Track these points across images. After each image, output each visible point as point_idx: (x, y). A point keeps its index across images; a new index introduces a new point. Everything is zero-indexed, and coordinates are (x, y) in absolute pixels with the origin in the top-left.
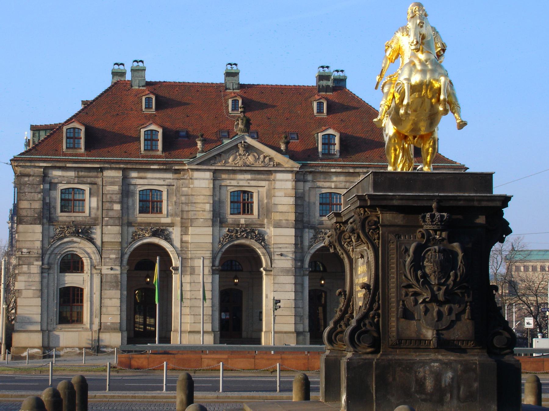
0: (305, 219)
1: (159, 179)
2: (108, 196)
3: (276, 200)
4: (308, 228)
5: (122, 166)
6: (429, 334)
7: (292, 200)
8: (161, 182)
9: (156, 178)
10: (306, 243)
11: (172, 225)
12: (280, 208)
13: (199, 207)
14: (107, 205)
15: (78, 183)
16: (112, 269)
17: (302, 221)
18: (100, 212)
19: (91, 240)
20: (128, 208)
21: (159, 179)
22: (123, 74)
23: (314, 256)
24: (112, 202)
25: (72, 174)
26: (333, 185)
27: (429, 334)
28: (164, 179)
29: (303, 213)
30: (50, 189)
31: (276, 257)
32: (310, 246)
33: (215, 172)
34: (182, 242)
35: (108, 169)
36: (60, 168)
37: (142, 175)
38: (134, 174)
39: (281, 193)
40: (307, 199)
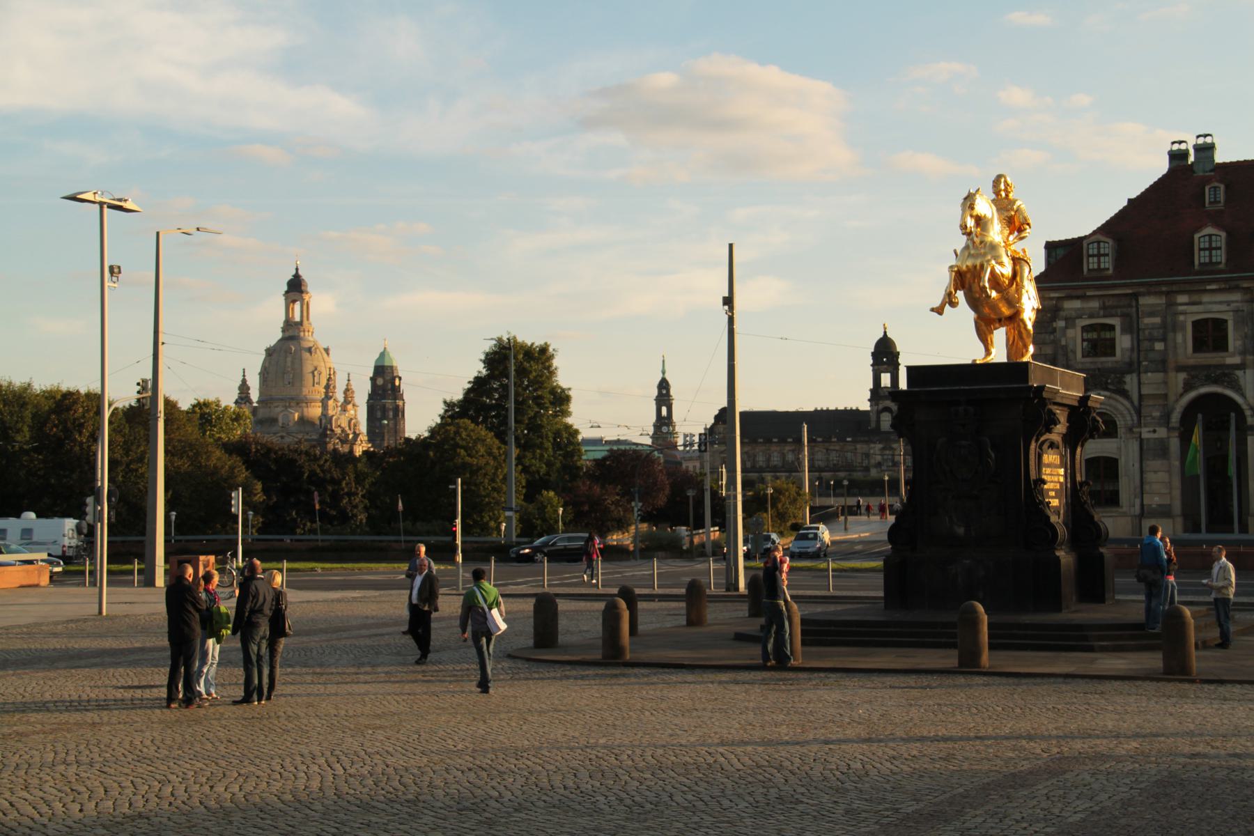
1: (1221, 303)
2: (1147, 332)
5: (1164, 289)
6: (961, 531)
8: (1224, 307)
9: (1215, 303)
14: (1145, 345)
15: (1105, 316)
16: (1154, 431)
18: (1135, 355)
19: (1125, 394)
20: (1175, 347)
21: (1221, 303)
22: (1185, 154)
24: (1152, 340)
25: (1095, 304)
27: (961, 531)
28: (1228, 303)
30: (1066, 327)
35: (1144, 294)
36: (1078, 298)
37: (1195, 298)
38: (1182, 299)
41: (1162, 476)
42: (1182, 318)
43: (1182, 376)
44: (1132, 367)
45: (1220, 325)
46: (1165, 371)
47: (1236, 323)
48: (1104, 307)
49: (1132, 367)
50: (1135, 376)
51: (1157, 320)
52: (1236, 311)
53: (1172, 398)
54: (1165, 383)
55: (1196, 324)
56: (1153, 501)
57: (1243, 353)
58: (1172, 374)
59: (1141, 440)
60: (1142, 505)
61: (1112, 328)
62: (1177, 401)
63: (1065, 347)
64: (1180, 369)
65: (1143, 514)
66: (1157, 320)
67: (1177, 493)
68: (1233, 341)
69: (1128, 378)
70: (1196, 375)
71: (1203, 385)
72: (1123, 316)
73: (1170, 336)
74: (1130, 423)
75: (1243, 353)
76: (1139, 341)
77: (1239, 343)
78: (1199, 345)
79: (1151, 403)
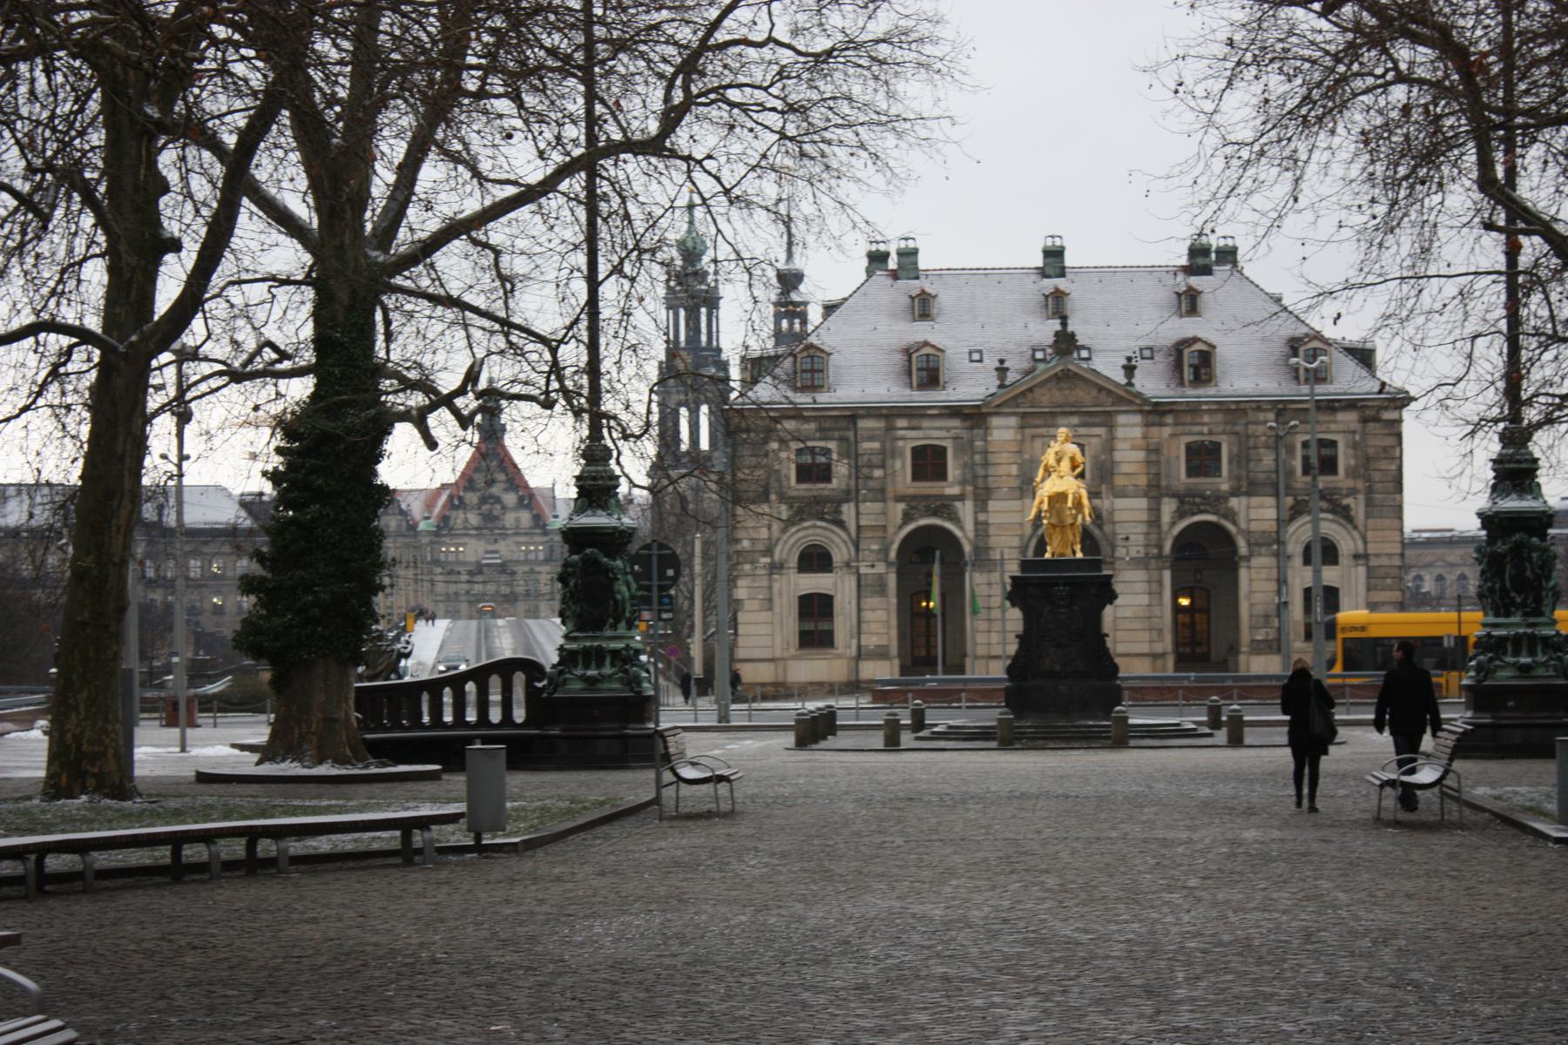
0: (1163, 483)
1: (940, 429)
3: (1118, 456)
4: (1168, 495)
7: (1141, 455)
8: (943, 434)
10: (1166, 518)
11: (961, 498)
12: (1125, 468)
13: (1002, 470)
17: (1158, 486)
18: (853, 483)
19: (841, 524)
23: (1177, 539)
24: (871, 466)
25: (812, 426)
26: (1205, 429)
28: (948, 429)
29: (1158, 474)
30: (780, 450)
31: (1120, 543)
32: (1173, 524)
33: (1024, 415)
34: (977, 523)
37: (915, 423)
38: (902, 423)
39: (1127, 445)
40: (1165, 452)
41: (881, 615)
42: (901, 443)
43: (901, 506)
44: (849, 495)
45: (940, 452)
46: (884, 500)
47: (956, 452)
48: (820, 430)
49: (849, 495)
50: (852, 504)
51: (876, 445)
52: (955, 438)
53: (891, 530)
54: (884, 513)
55: (915, 450)
56: (870, 641)
57: (963, 483)
58: (891, 504)
59: (859, 576)
60: (859, 647)
61: (827, 452)
62: (895, 534)
63: (778, 472)
64: (899, 499)
65: (859, 657)
66: (876, 445)
67: (894, 633)
68: (953, 470)
69: (845, 508)
70: (915, 505)
71: (922, 516)
72: (842, 439)
73: (889, 462)
74: (846, 557)
75: (963, 483)
76: (857, 468)
77: (958, 472)
78: (917, 475)
79: (870, 534)
